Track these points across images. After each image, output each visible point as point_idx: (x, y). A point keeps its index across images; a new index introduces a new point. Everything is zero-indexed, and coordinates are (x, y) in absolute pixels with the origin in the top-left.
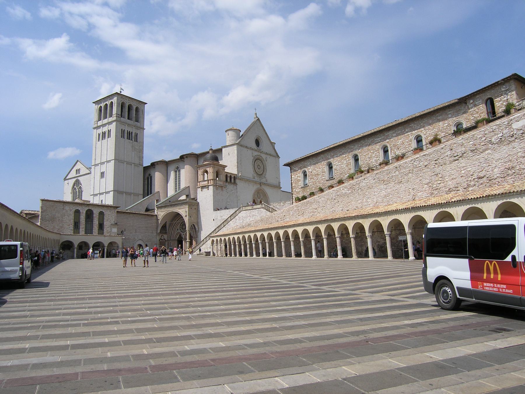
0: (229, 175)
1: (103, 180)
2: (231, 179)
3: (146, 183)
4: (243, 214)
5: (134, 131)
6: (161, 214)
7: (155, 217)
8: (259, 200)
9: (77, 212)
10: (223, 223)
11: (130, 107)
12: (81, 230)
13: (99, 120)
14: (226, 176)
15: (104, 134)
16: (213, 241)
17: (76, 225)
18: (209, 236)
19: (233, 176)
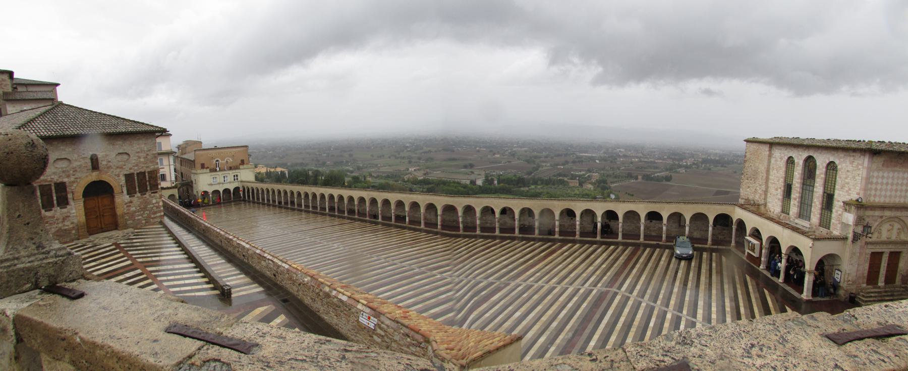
9: (790, 161)
12: (792, 202)
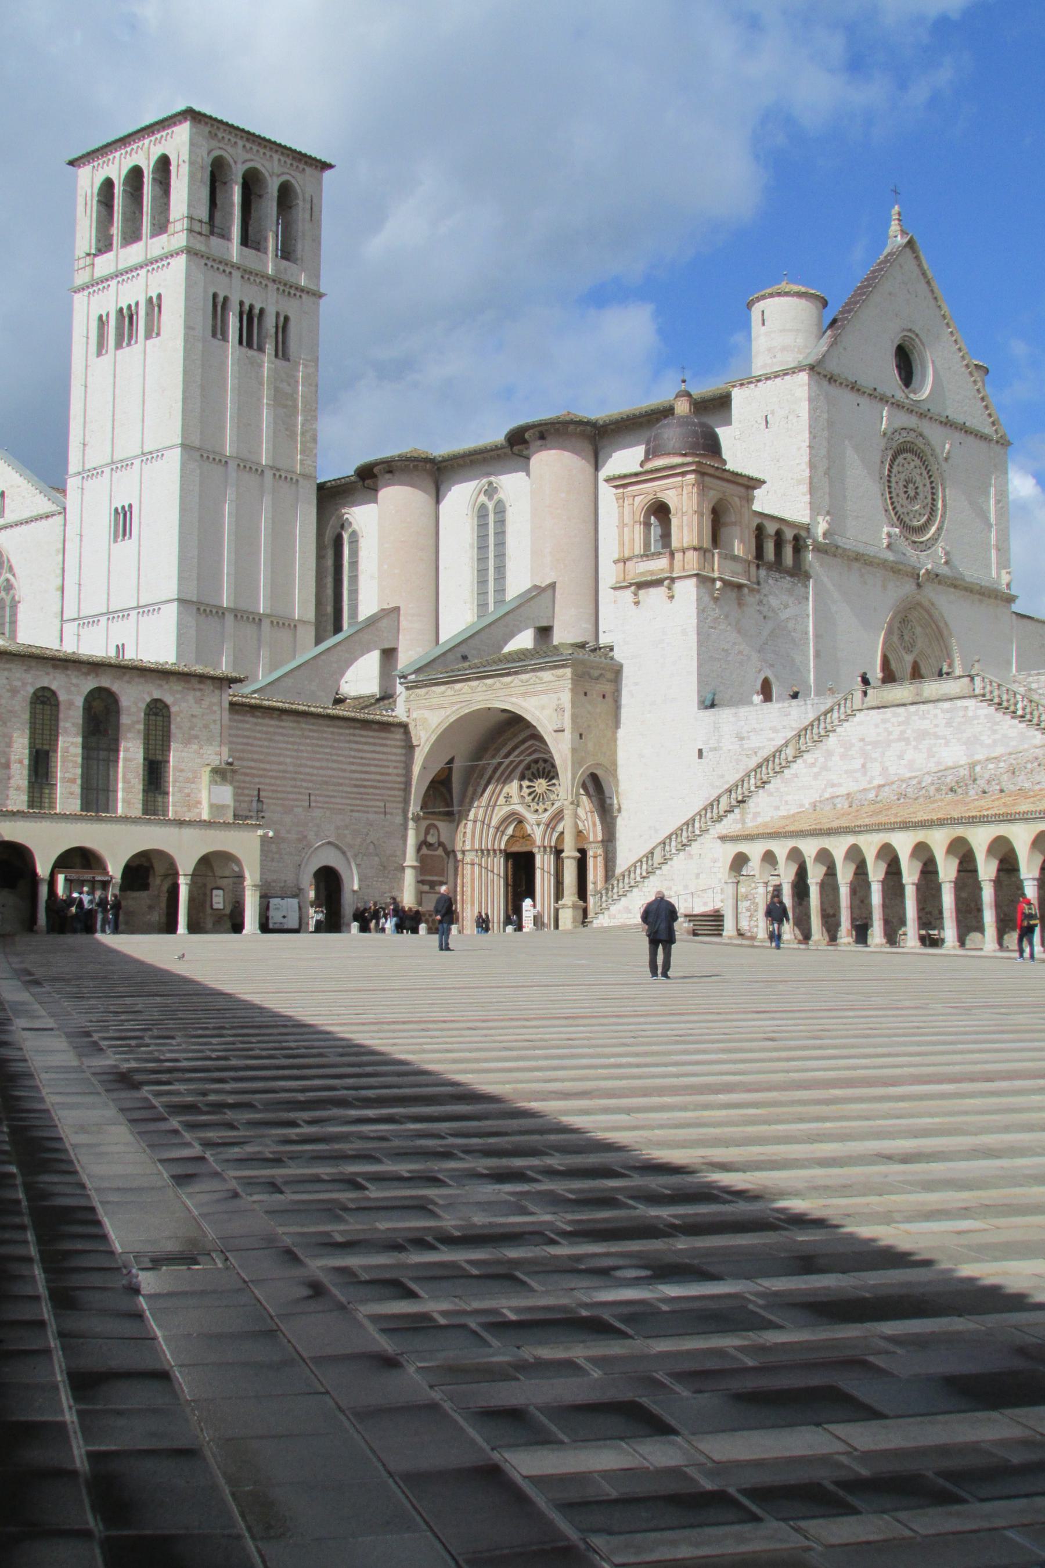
0: (771, 528)
1: (127, 547)
2: (781, 551)
3: (330, 562)
4: (865, 725)
5: (271, 303)
6: (430, 716)
7: (399, 735)
8: (909, 659)
9: (45, 702)
10: (760, 766)
11: (252, 184)
13: (100, 252)
14: (760, 530)
15: (127, 317)
16: (740, 862)
17: (41, 765)
18: (684, 837)
19: (789, 534)
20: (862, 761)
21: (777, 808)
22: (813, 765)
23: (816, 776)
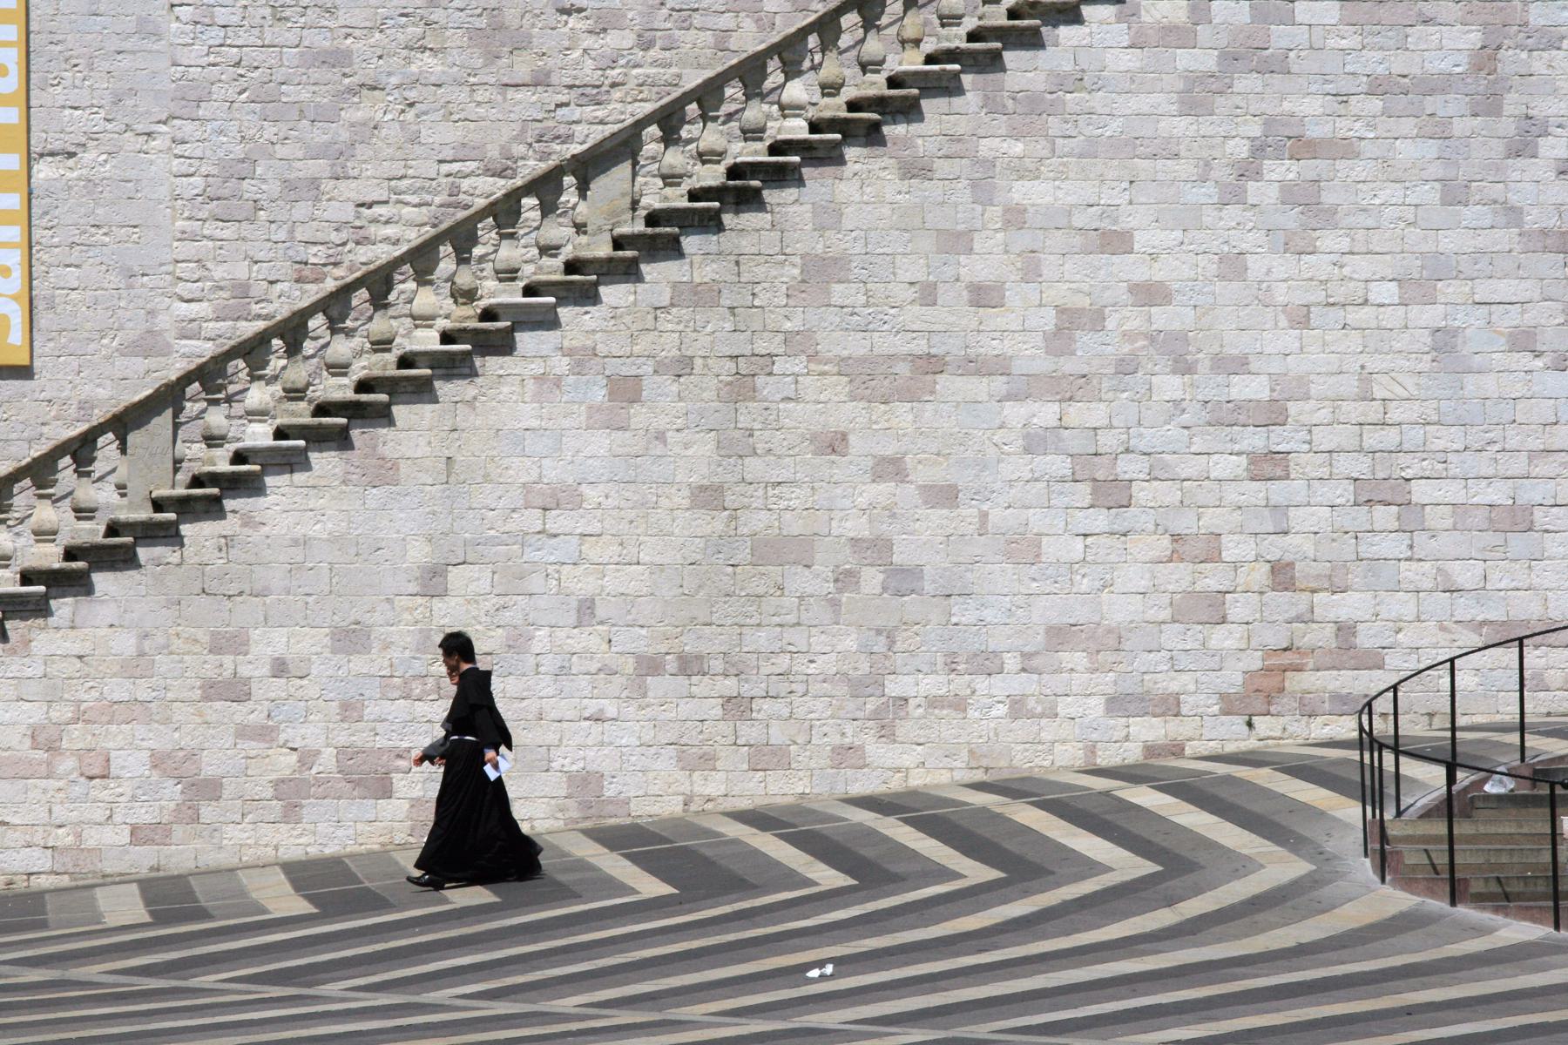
20: (1474, 38)
21: (958, 242)
22: (1176, 36)
23: (1197, 96)
